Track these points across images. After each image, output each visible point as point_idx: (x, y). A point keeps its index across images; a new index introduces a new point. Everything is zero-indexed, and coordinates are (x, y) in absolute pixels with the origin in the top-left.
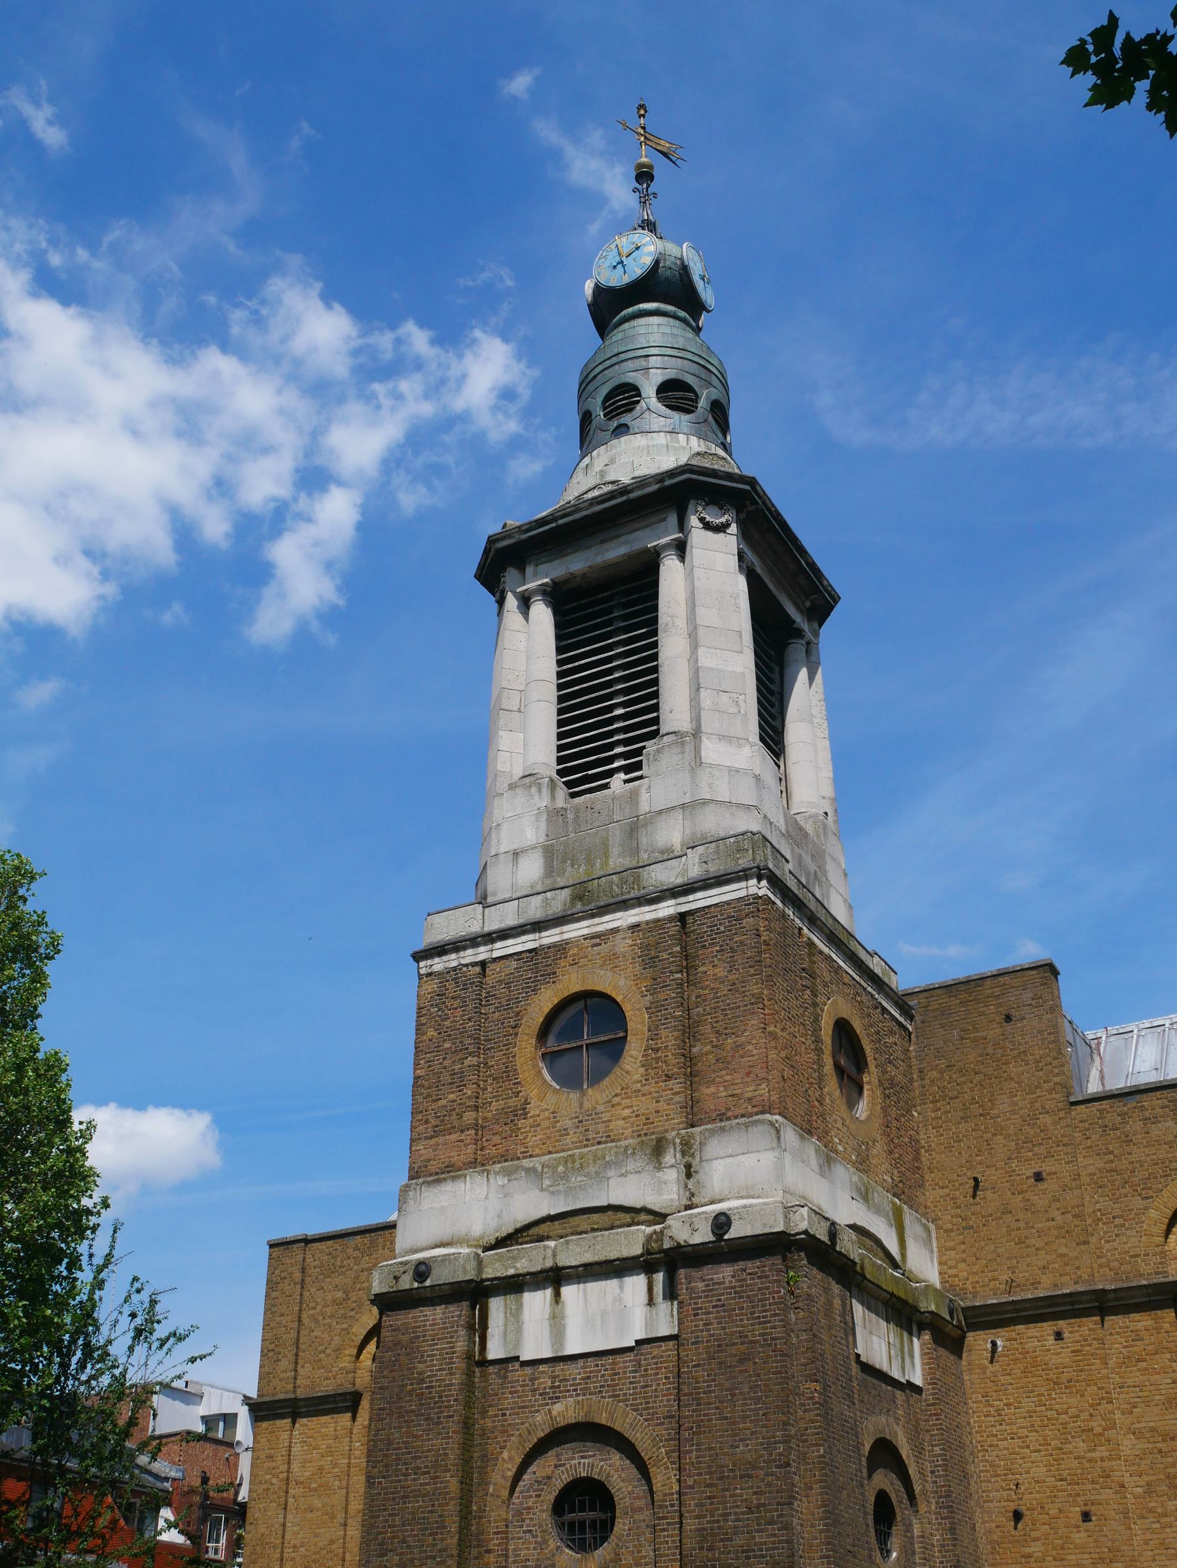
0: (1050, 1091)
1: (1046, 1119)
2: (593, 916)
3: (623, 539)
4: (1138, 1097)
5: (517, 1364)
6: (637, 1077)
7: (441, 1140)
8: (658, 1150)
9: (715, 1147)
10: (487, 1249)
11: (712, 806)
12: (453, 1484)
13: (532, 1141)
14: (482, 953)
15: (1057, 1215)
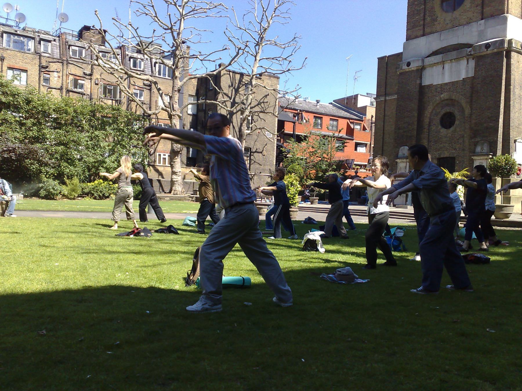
6: (468, 6)
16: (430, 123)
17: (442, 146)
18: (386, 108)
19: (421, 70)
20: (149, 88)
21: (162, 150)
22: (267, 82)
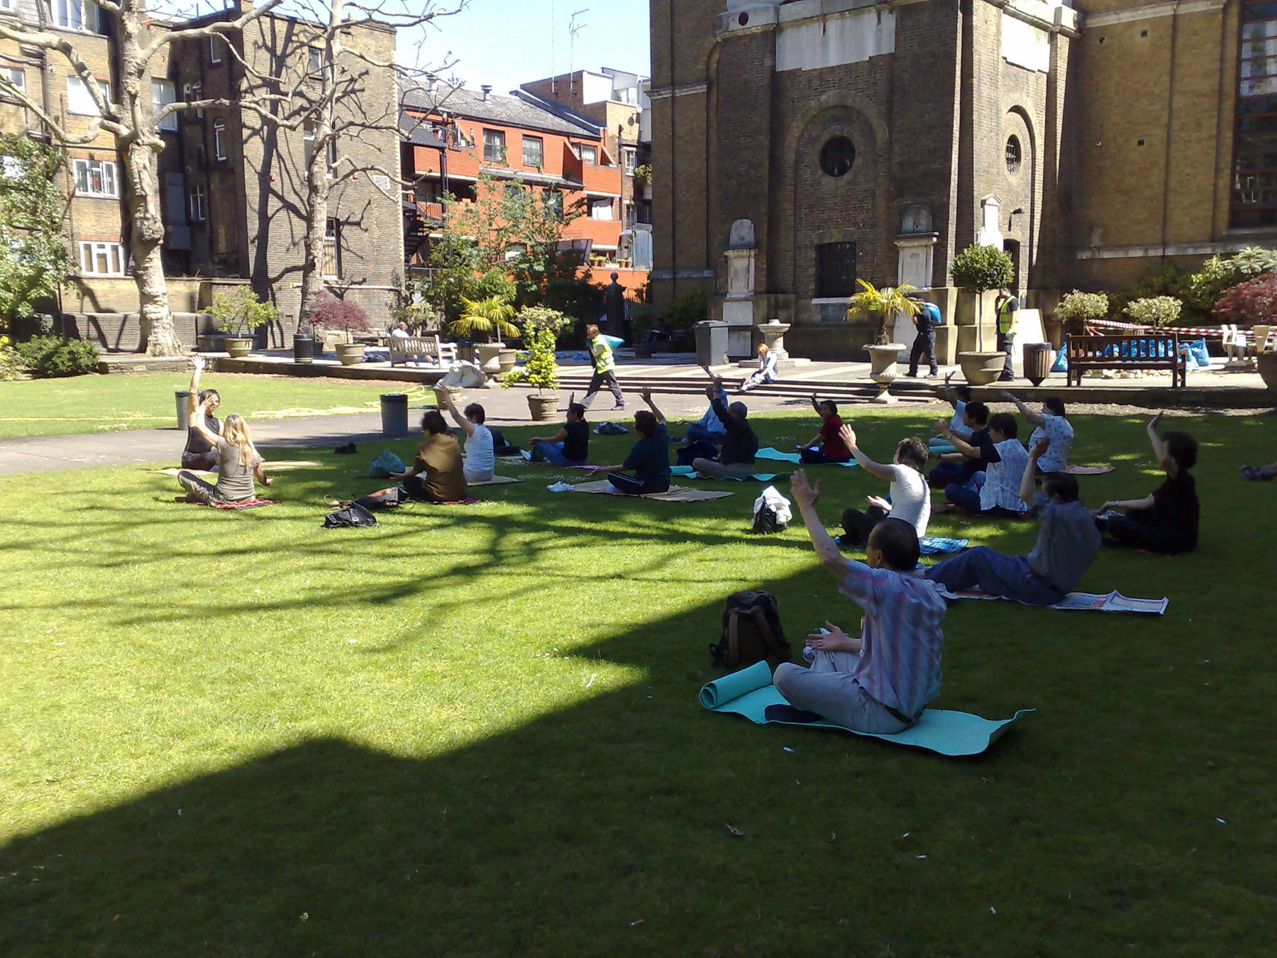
12: (765, 142)
16: (796, 162)
17: (825, 216)
18: (677, 117)
19: (772, 34)
20: (37, 62)
21: (92, 232)
22: (363, 41)
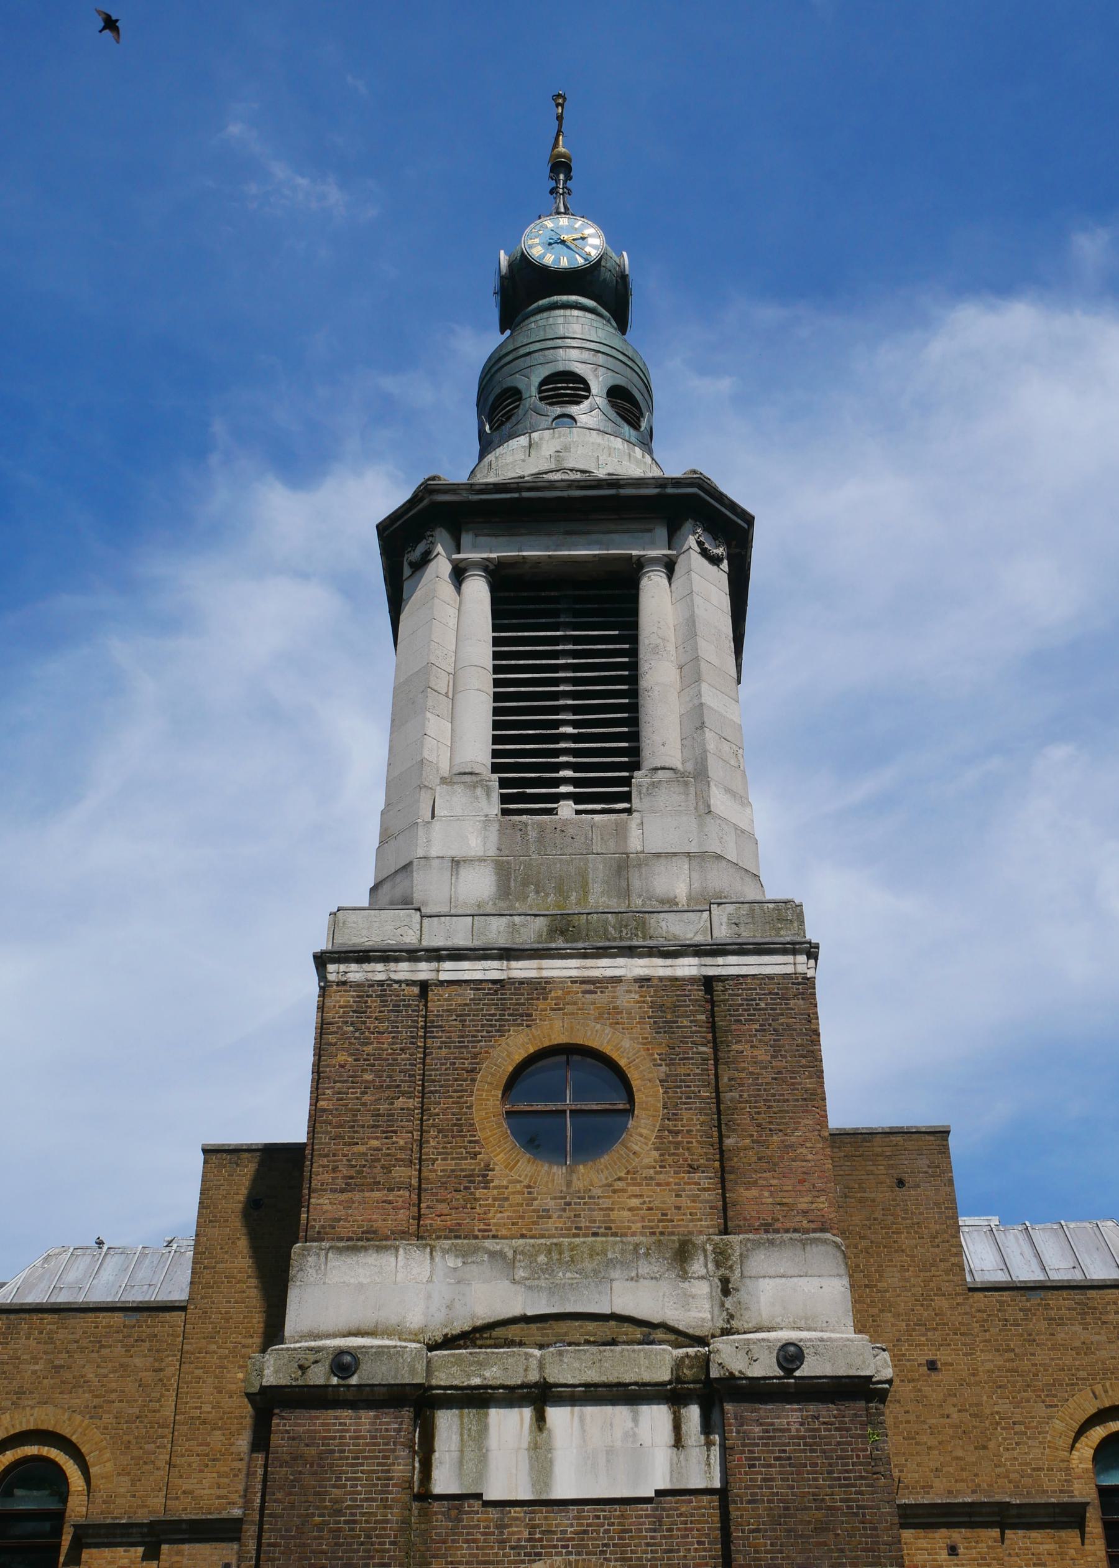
0: (947, 1272)
1: (942, 1303)
2: (585, 956)
3: (594, 537)
4: (1042, 1293)
5: (477, 1505)
7: (357, 1196)
8: (682, 1254)
9: (760, 1261)
10: (431, 1348)
11: (724, 863)
13: (496, 1218)
14: (424, 971)
15: (952, 1411)
